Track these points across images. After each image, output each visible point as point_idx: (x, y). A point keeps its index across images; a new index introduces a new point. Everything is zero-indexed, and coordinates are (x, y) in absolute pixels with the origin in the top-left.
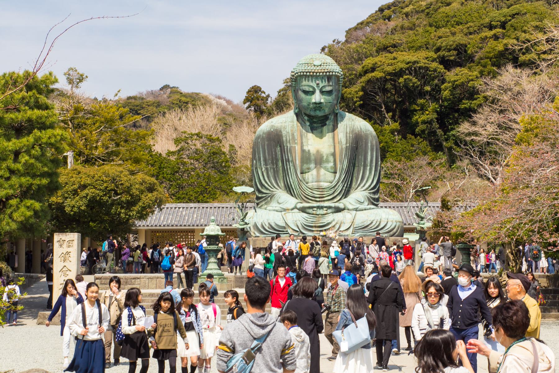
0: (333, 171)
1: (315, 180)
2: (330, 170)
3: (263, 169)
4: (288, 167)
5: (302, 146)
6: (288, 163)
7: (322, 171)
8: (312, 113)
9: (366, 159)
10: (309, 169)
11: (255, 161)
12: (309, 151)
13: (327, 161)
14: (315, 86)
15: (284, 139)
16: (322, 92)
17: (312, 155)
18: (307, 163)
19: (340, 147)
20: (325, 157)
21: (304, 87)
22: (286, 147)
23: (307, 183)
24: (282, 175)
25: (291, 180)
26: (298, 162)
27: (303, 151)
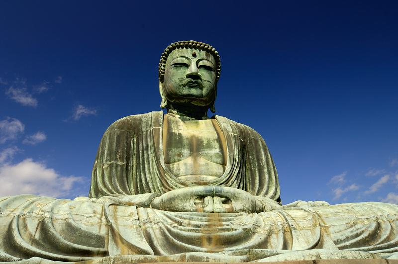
0: (219, 160)
1: (190, 172)
2: (215, 159)
3: (106, 166)
4: (146, 157)
5: (169, 128)
6: (145, 152)
7: (202, 161)
8: (185, 91)
9: (259, 159)
10: (180, 155)
11: (96, 162)
12: (180, 135)
13: (209, 146)
14: (191, 57)
15: (144, 124)
16: (200, 67)
17: (184, 138)
18: (177, 147)
19: (226, 134)
20: (205, 142)
21: (176, 60)
22: (144, 133)
23: (177, 176)
24: (134, 176)
25: (147, 175)
26: (161, 146)
27: (170, 134)
